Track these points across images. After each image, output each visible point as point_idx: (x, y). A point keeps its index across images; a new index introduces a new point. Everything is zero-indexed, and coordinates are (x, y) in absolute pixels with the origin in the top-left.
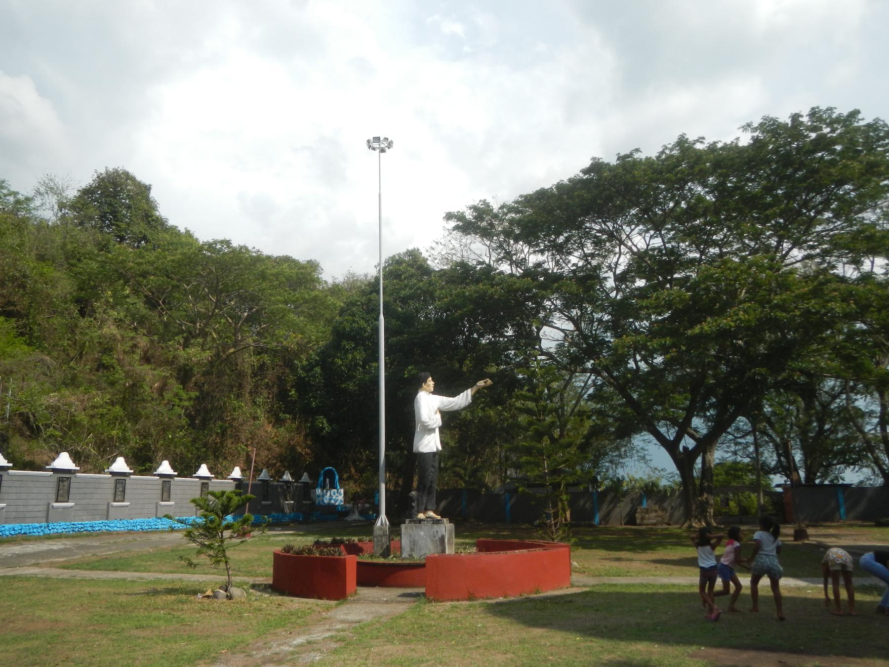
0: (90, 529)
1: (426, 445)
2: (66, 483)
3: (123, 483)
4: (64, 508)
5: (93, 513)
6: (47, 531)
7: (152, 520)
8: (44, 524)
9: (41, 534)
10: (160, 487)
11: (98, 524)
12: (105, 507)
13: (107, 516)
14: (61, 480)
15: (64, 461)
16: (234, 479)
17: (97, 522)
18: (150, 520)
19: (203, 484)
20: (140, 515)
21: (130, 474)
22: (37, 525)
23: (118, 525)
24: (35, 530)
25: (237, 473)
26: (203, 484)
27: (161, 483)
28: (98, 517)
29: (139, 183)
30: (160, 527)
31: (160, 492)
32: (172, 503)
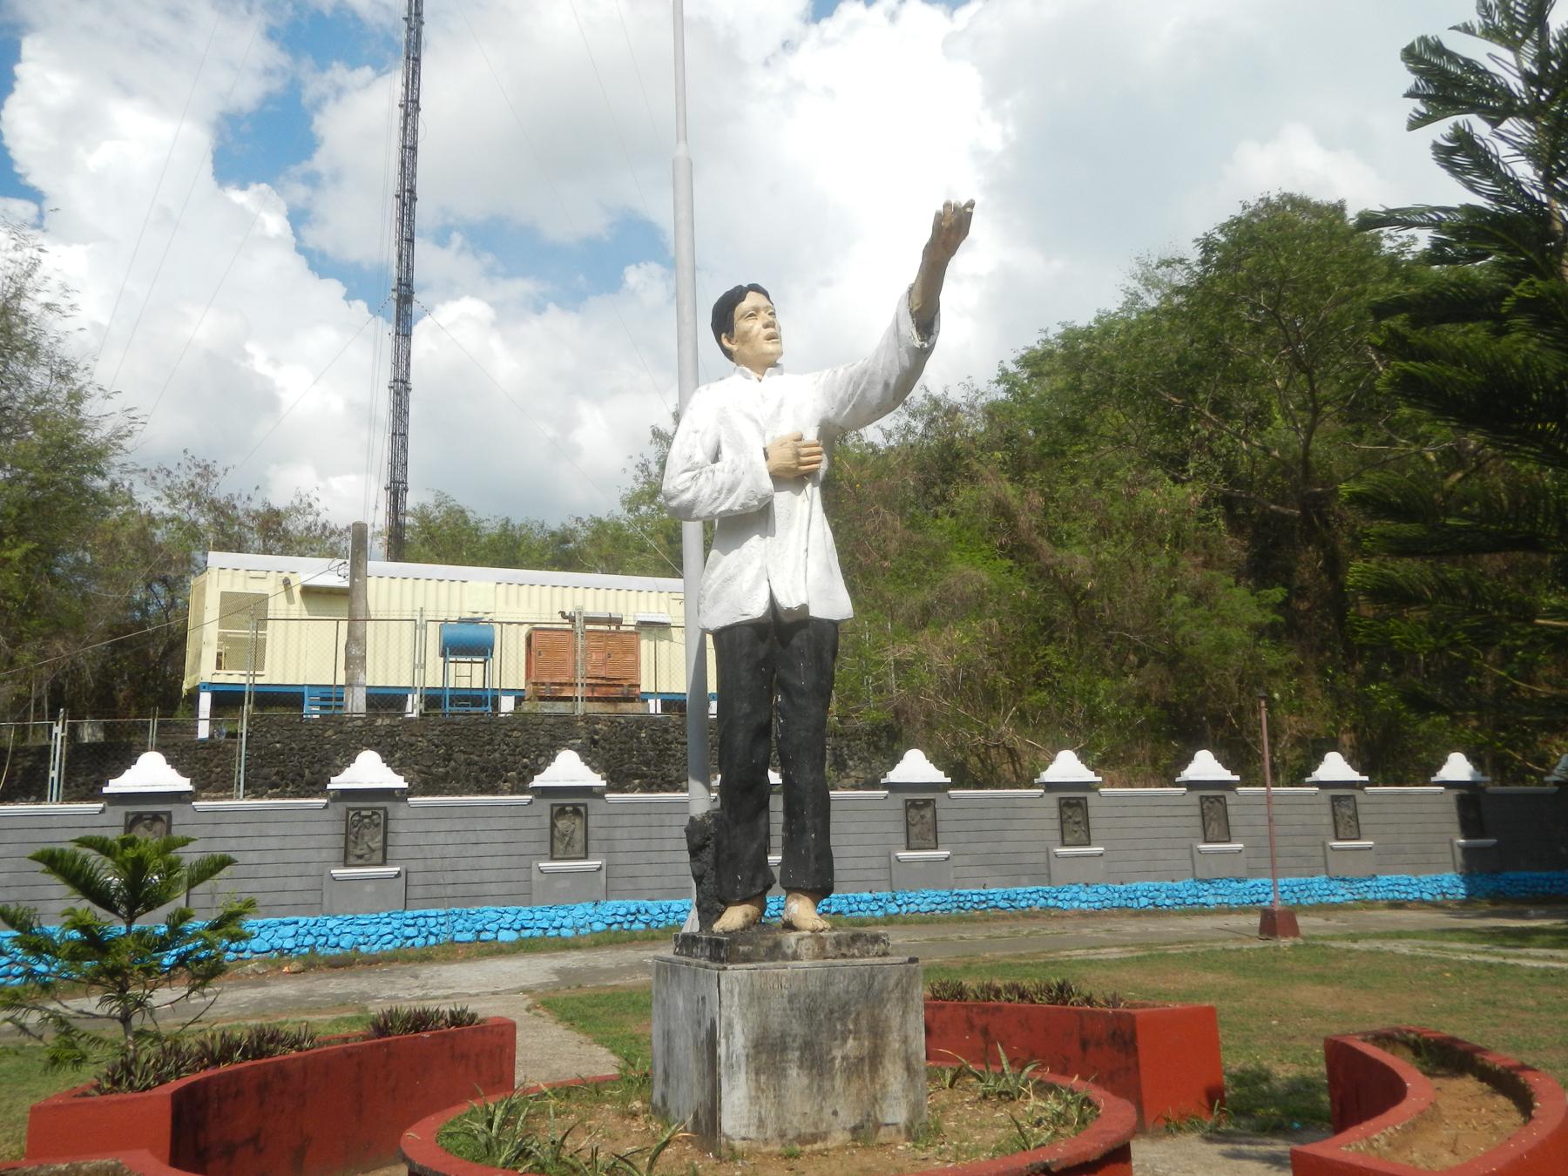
0: (1002, 904)
1: (716, 599)
2: (928, 813)
3: (1081, 804)
4: (928, 861)
5: (1015, 871)
6: (893, 909)
7: (1185, 886)
8: (885, 895)
9: (879, 913)
10: (1197, 811)
11: (1027, 893)
12: (1042, 858)
13: (1049, 876)
14: (912, 805)
15: (1067, 767)
16: (1448, 785)
17: (1020, 890)
18: (1179, 885)
19: (1335, 799)
20: (1145, 874)
21: (1101, 785)
22: (867, 896)
23: (1083, 896)
24: (862, 906)
25: (1458, 767)
26: (1335, 799)
27: (1196, 800)
28: (1025, 879)
29: (1317, 206)
30: (1211, 900)
31: (1198, 821)
32: (943, 853)
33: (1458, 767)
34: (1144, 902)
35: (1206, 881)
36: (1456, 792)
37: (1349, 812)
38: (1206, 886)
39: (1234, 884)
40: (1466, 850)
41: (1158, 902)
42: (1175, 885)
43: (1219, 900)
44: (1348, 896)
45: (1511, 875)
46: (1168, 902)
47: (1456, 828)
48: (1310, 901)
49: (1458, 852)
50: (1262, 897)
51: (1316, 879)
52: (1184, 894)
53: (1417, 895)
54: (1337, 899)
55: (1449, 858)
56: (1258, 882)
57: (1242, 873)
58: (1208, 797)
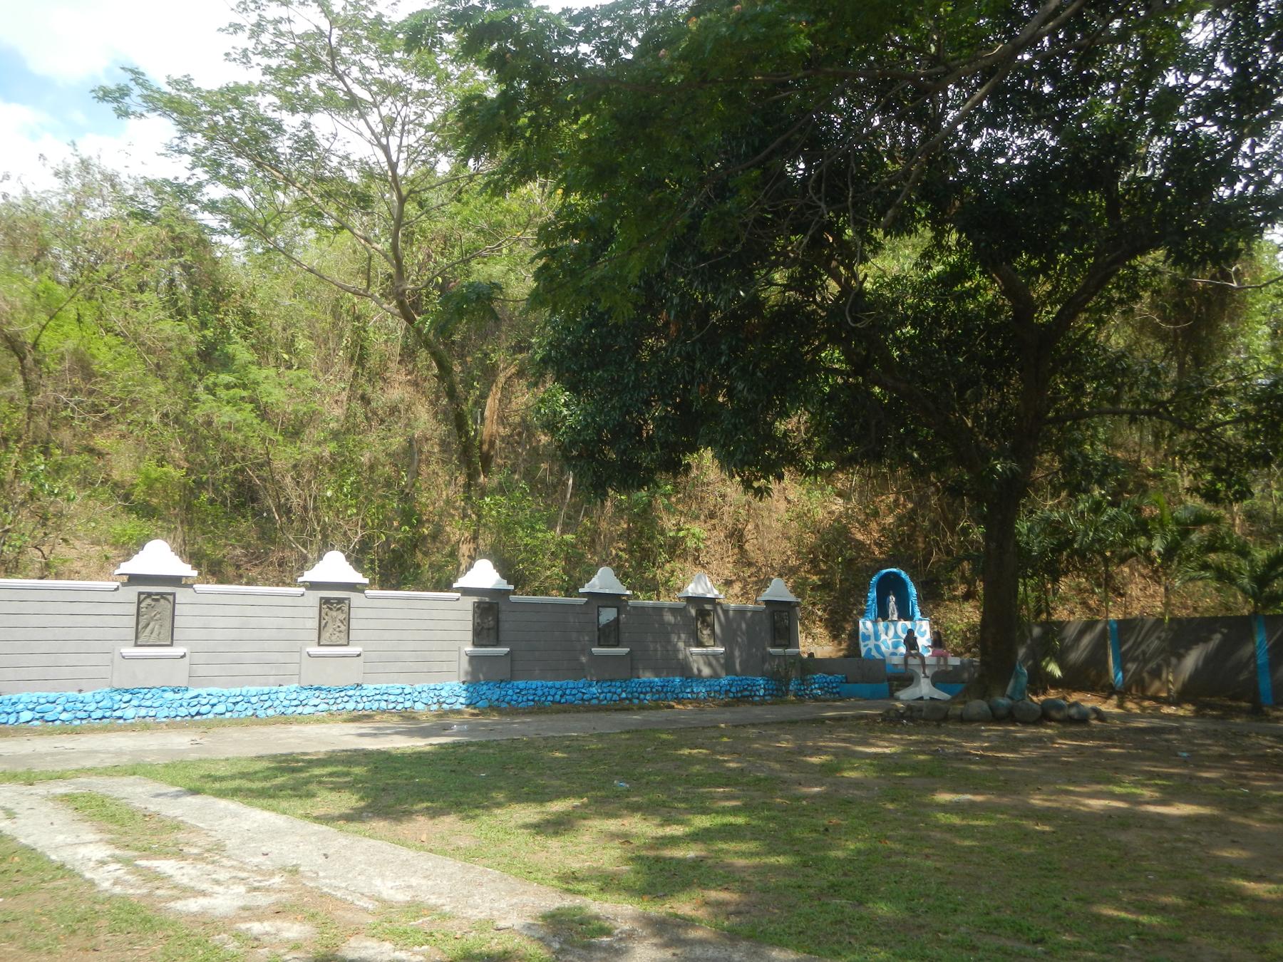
10: (133, 609)
26: (326, 601)
30: (130, 713)
33: (484, 575)
34: (26, 716)
35: (127, 691)
36: (475, 599)
37: (342, 616)
38: (127, 697)
39: (169, 695)
40: (473, 659)
41: (48, 716)
42: (80, 696)
43: (143, 712)
44: (323, 707)
45: (521, 684)
46: (64, 716)
47: (470, 636)
48: (271, 712)
49: (465, 660)
50: (203, 710)
51: (283, 689)
52: (92, 707)
53: (408, 704)
54: (307, 710)
55: (454, 666)
56: (203, 692)
57: (181, 681)
58: (149, 595)
